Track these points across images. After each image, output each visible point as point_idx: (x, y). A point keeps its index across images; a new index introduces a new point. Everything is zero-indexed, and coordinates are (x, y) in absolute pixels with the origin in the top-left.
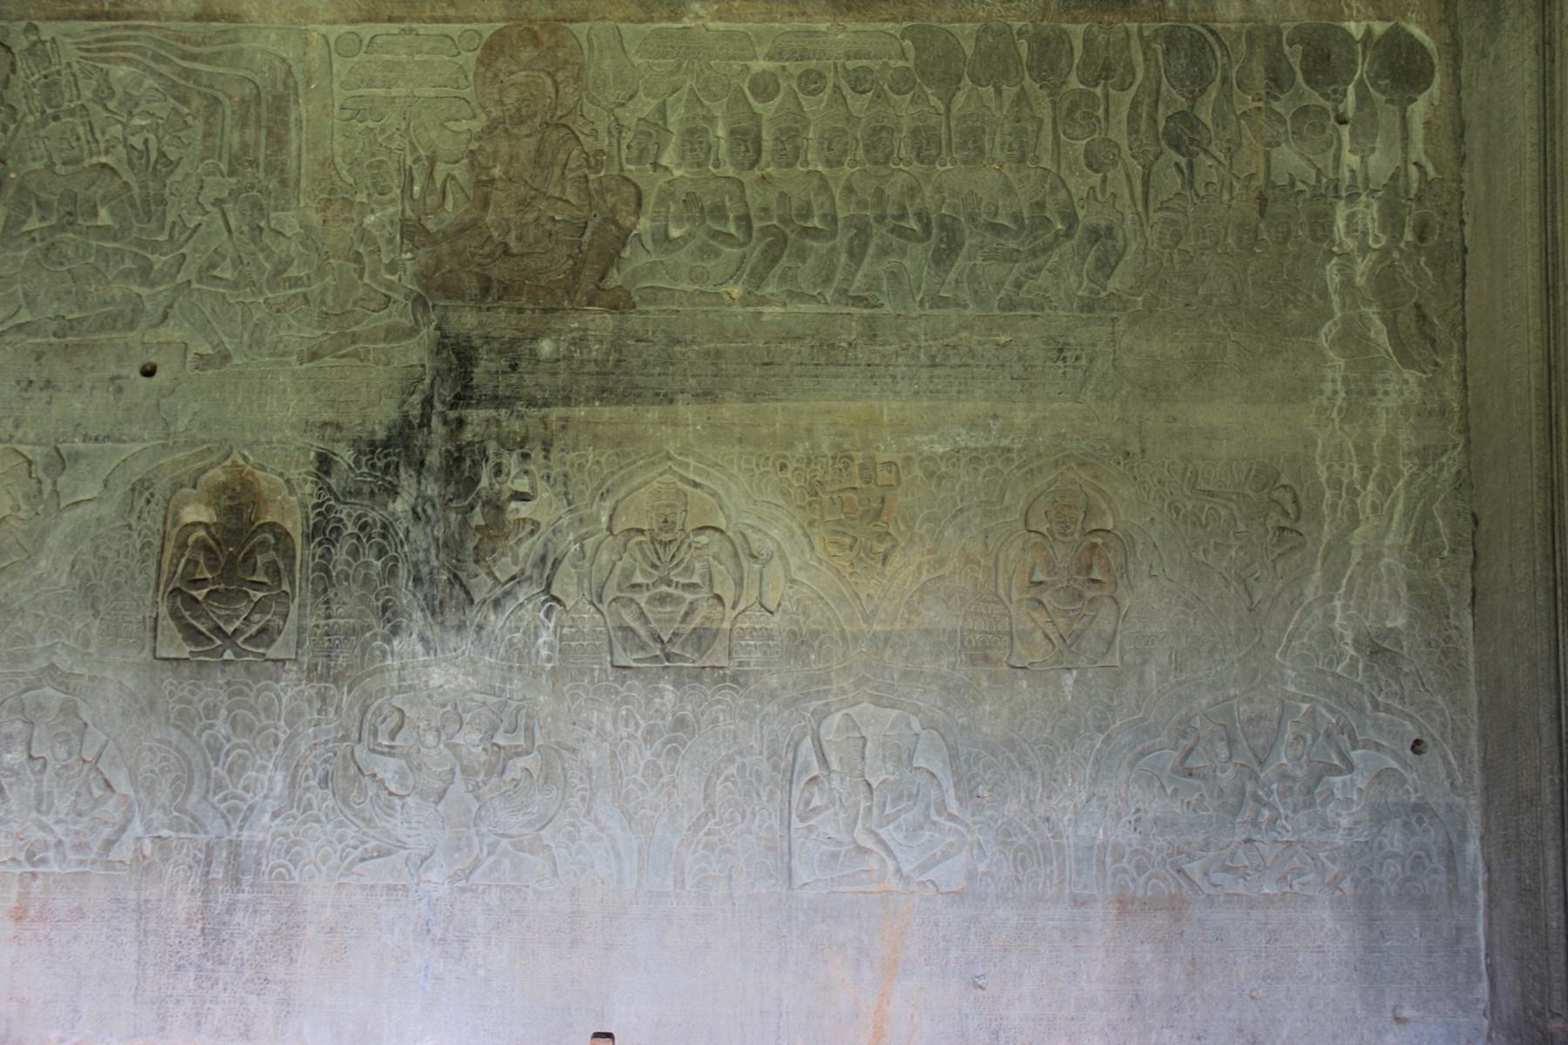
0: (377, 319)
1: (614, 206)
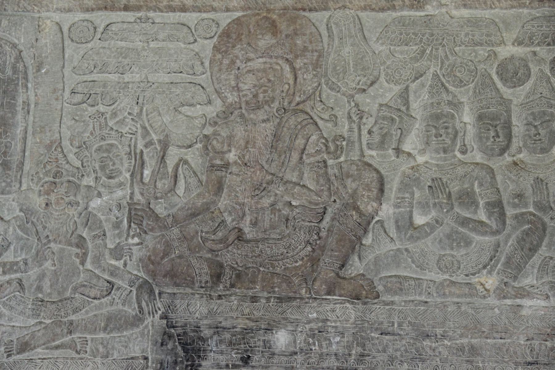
0: (98, 308)
1: (355, 191)
